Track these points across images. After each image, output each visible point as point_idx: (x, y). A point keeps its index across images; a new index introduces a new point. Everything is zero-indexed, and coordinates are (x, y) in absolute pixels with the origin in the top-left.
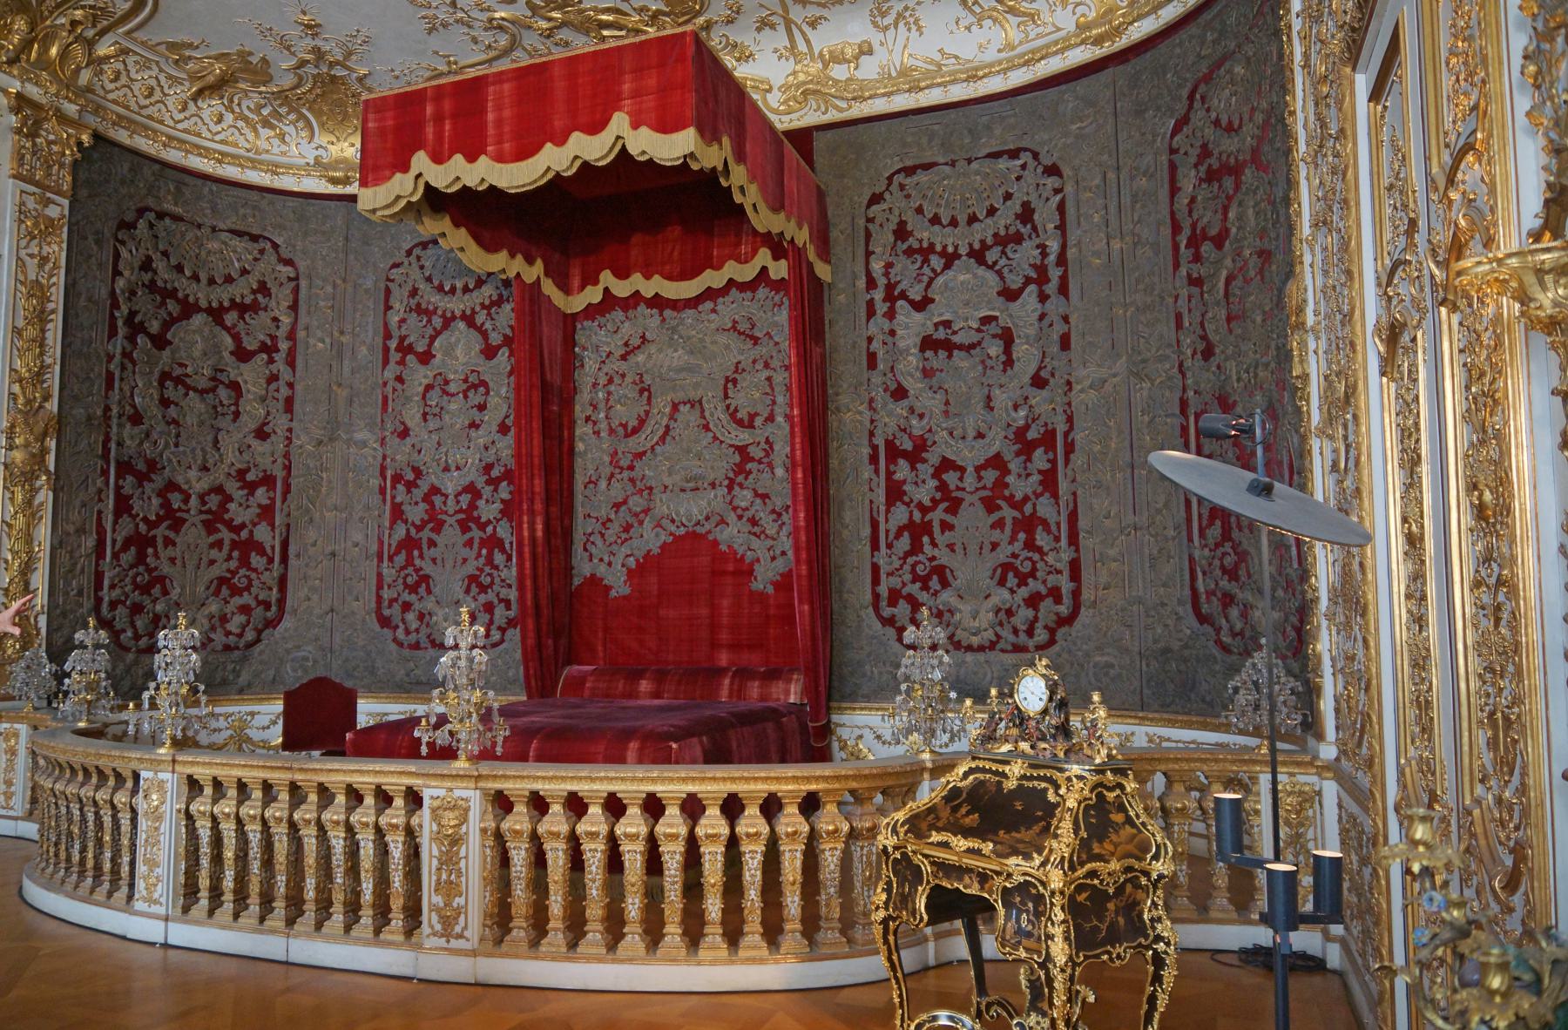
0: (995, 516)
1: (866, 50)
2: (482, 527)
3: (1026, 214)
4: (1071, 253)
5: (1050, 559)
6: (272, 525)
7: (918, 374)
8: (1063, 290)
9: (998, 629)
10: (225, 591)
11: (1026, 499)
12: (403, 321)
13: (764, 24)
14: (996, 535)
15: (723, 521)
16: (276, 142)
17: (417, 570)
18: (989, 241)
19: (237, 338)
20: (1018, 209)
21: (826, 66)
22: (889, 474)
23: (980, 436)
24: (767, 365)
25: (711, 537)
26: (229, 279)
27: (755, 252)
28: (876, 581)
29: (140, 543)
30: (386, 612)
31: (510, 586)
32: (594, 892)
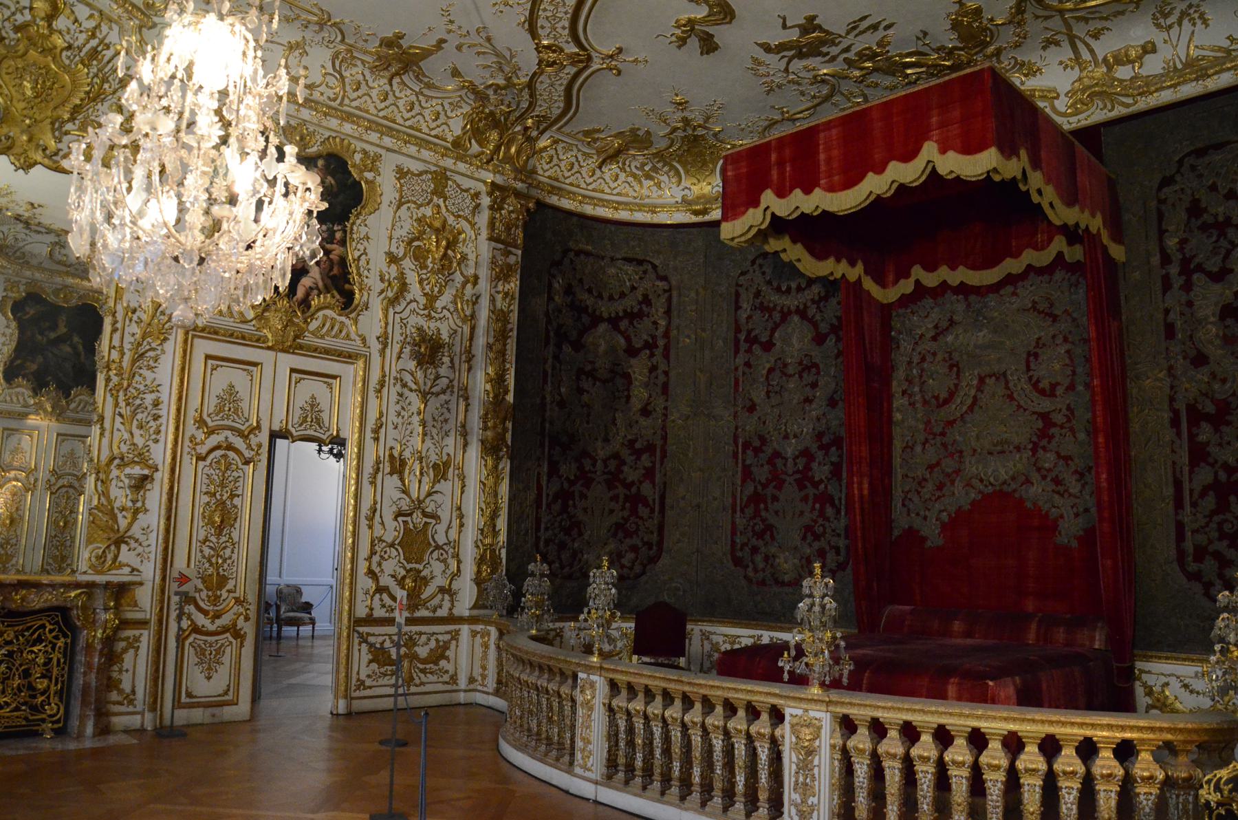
1: (1149, 48)
2: (816, 485)
6: (653, 483)
7: (1218, 342)
10: (620, 535)
12: (749, 317)
13: (1049, 43)
15: (1028, 481)
16: (655, 188)
17: (763, 520)
19: (628, 339)
21: (1110, 68)
22: (1192, 437)
24: (1066, 340)
26: (623, 295)
27: (1050, 240)
28: (1180, 537)
29: (564, 496)
30: (739, 554)
31: (839, 535)
32: (925, 807)
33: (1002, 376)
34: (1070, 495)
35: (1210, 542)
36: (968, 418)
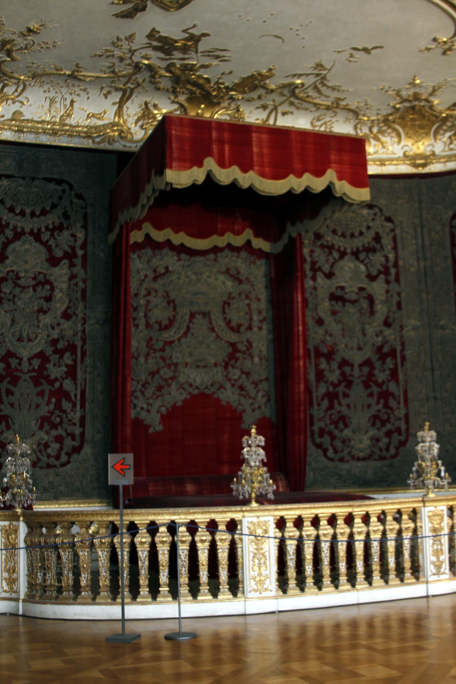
0: (369, 390)
2: (52, 383)
3: (378, 238)
4: (401, 263)
5: (396, 413)
7: (329, 313)
8: (397, 280)
9: (373, 448)
11: (383, 382)
14: (370, 400)
15: (222, 387)
18: (361, 248)
20: (374, 235)
22: (317, 365)
23: (360, 349)
24: (247, 297)
25: (215, 396)
31: (75, 424)
33: (205, 314)
34: (250, 397)
35: (326, 426)
36: (183, 340)
